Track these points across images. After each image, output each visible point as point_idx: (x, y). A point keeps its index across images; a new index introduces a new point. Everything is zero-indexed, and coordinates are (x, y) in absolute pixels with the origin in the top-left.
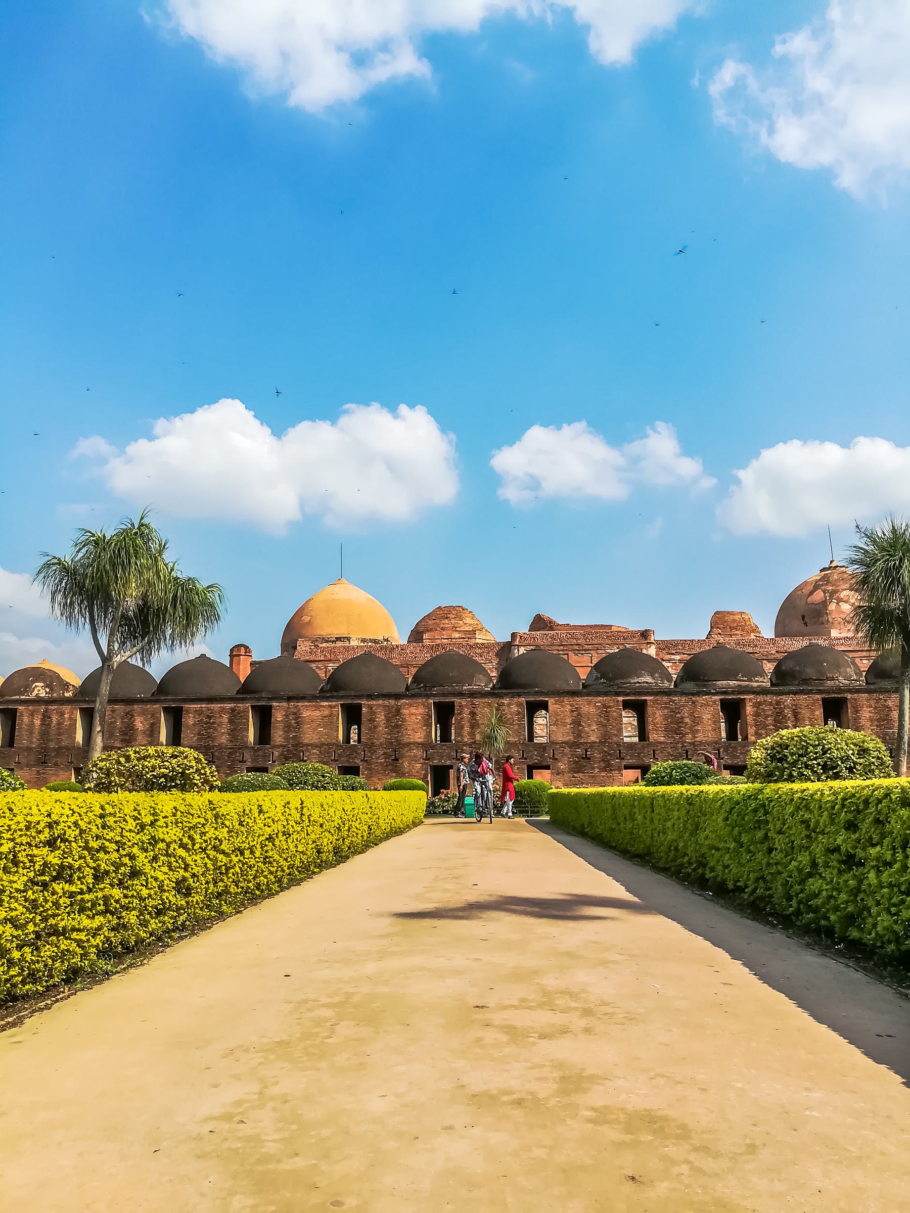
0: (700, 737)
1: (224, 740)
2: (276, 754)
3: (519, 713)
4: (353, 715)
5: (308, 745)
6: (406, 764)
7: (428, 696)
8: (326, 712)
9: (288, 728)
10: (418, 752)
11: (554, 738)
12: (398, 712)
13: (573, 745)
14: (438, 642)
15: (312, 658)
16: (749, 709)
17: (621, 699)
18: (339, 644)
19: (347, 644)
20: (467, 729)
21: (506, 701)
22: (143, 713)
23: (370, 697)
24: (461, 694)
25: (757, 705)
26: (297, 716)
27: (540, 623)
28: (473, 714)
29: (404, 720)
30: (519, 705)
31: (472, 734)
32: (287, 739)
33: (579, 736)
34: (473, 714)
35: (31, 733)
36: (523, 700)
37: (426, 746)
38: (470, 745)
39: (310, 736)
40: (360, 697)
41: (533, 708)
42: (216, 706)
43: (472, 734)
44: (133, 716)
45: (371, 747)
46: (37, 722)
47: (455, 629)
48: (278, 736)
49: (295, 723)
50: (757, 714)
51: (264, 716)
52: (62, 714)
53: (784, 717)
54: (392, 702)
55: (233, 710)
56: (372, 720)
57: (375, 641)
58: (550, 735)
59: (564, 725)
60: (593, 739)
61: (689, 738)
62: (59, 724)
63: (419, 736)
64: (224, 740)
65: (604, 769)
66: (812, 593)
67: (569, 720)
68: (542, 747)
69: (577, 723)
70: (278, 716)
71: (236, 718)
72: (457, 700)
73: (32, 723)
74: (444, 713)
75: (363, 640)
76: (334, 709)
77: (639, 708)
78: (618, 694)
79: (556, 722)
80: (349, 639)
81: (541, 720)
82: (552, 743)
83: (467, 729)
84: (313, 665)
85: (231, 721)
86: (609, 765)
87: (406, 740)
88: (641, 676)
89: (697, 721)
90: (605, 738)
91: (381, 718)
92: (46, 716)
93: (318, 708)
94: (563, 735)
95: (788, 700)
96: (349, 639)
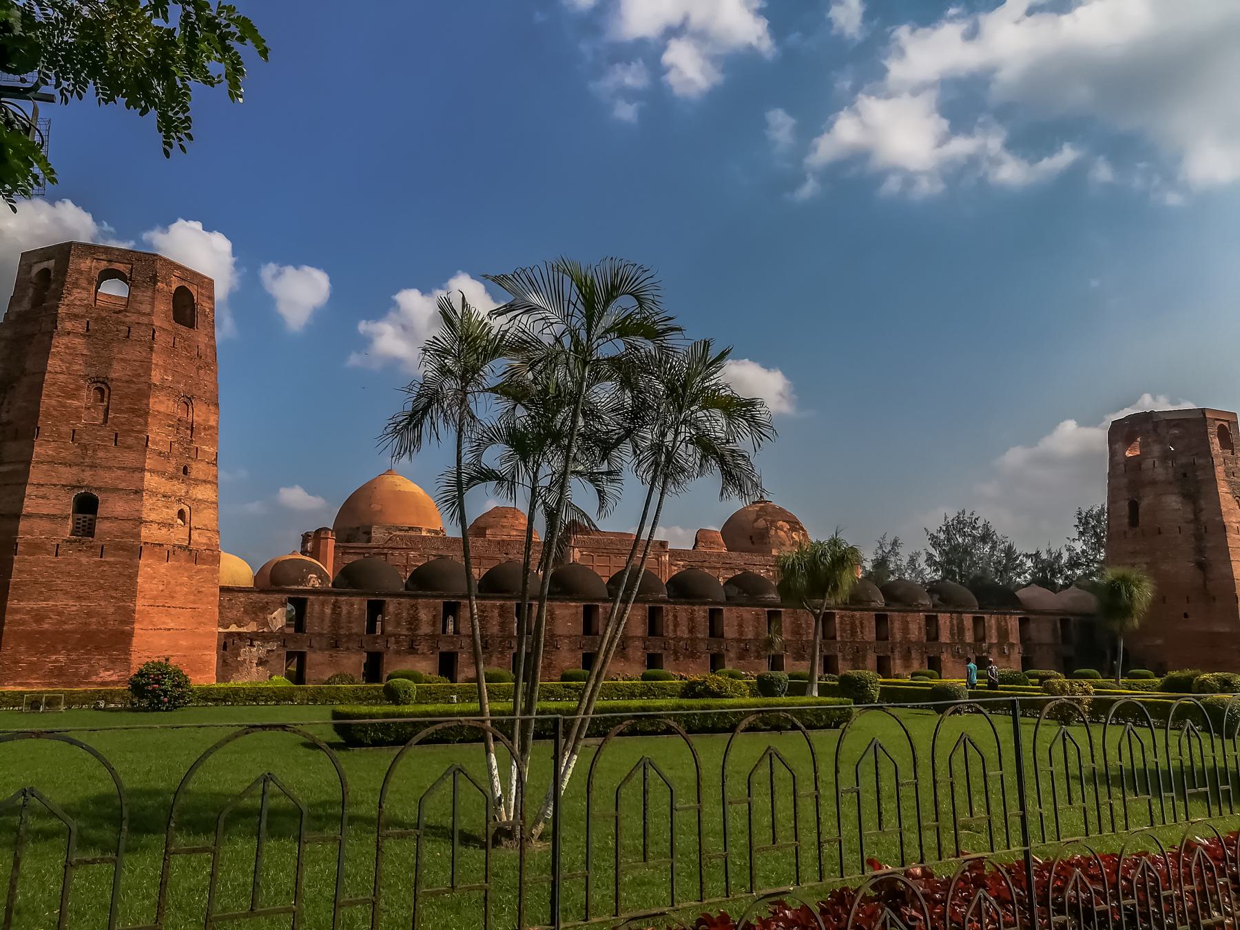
1: (494, 629)
7: (645, 602)
8: (574, 611)
13: (739, 641)
16: (837, 620)
18: (412, 533)
21: (696, 608)
22: (426, 606)
25: (842, 617)
28: (675, 617)
30: (705, 611)
31: (675, 631)
34: (675, 617)
35: (323, 620)
43: (675, 631)
46: (328, 611)
50: (841, 623)
52: (352, 605)
55: (502, 606)
60: (750, 636)
62: (349, 613)
65: (757, 658)
66: (756, 520)
69: (740, 625)
73: (323, 612)
75: (429, 531)
80: (420, 530)
84: (396, 553)
85: (500, 615)
90: (757, 634)
92: (336, 606)
93: (568, 607)
95: (858, 614)
96: (420, 530)
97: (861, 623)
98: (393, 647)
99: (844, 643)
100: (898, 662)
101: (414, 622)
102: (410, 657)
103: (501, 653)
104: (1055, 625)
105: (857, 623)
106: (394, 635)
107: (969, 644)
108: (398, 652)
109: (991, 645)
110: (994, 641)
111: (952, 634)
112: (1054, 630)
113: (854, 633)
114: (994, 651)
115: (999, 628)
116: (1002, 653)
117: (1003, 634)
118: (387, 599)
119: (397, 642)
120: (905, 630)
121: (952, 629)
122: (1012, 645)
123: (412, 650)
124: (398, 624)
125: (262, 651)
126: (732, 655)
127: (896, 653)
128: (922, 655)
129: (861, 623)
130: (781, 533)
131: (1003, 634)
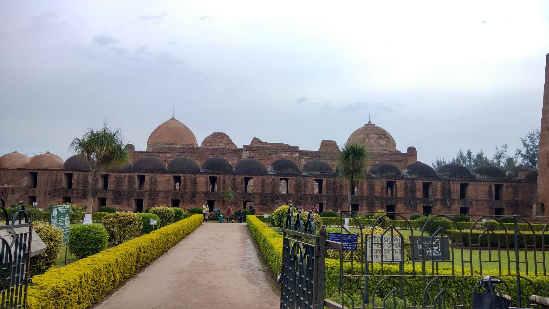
0: (307, 193)
1: (125, 188)
2: (147, 194)
3: (241, 182)
4: (177, 179)
5: (159, 191)
6: (198, 200)
9: (151, 184)
10: (203, 195)
11: (254, 191)
12: (195, 179)
13: (261, 194)
14: (213, 147)
15: (161, 151)
16: (324, 183)
17: (280, 177)
18: (172, 146)
19: (175, 146)
20: (222, 187)
21: (237, 177)
23: (184, 173)
24: (220, 174)
25: (327, 182)
26: (156, 180)
27: (255, 140)
28: (224, 182)
29: (197, 183)
31: (224, 189)
32: (151, 188)
33: (264, 191)
34: (224, 182)
36: (243, 177)
37: (206, 193)
38: (222, 193)
39: (160, 187)
40: (181, 173)
41: (247, 180)
42: (122, 174)
43: (224, 189)
44: (87, 177)
45: (184, 192)
47: (220, 142)
48: (147, 186)
49: (154, 182)
50: (327, 185)
51: (142, 179)
52: (57, 175)
53: (337, 187)
54: (193, 175)
56: (185, 183)
57: (187, 145)
58: (253, 189)
59: (258, 187)
60: (269, 192)
61: (302, 193)
62: (56, 179)
63: (203, 189)
64: (125, 188)
65: (272, 203)
67: (260, 185)
68: (250, 195)
70: (147, 179)
71: (131, 179)
72: (218, 176)
74: (213, 180)
76: (171, 177)
77: (287, 180)
78: (278, 176)
79: (255, 186)
81: (251, 182)
82: (253, 193)
83: (222, 187)
86: (274, 202)
87: (198, 191)
88: (288, 169)
89: (306, 186)
90: (273, 193)
91: (188, 182)
94: (258, 190)
97: (341, 186)
98: (75, 195)
99: (328, 197)
100: (365, 208)
101: (85, 183)
102: (83, 200)
103: (128, 199)
104: (490, 187)
105: (338, 185)
106: (76, 189)
107: (419, 199)
108: (77, 197)
109: (436, 200)
110: (439, 197)
111: (406, 193)
112: (490, 191)
113: (335, 190)
114: (439, 203)
115: (443, 190)
116: (444, 204)
117: (447, 193)
118: (73, 172)
119: (77, 193)
120: (371, 188)
121: (406, 189)
122: (454, 200)
123: (85, 197)
124: (78, 184)
125: (18, 196)
126: (257, 202)
127: (364, 202)
128: (382, 204)
129: (341, 186)
130: (372, 141)
131: (447, 193)
